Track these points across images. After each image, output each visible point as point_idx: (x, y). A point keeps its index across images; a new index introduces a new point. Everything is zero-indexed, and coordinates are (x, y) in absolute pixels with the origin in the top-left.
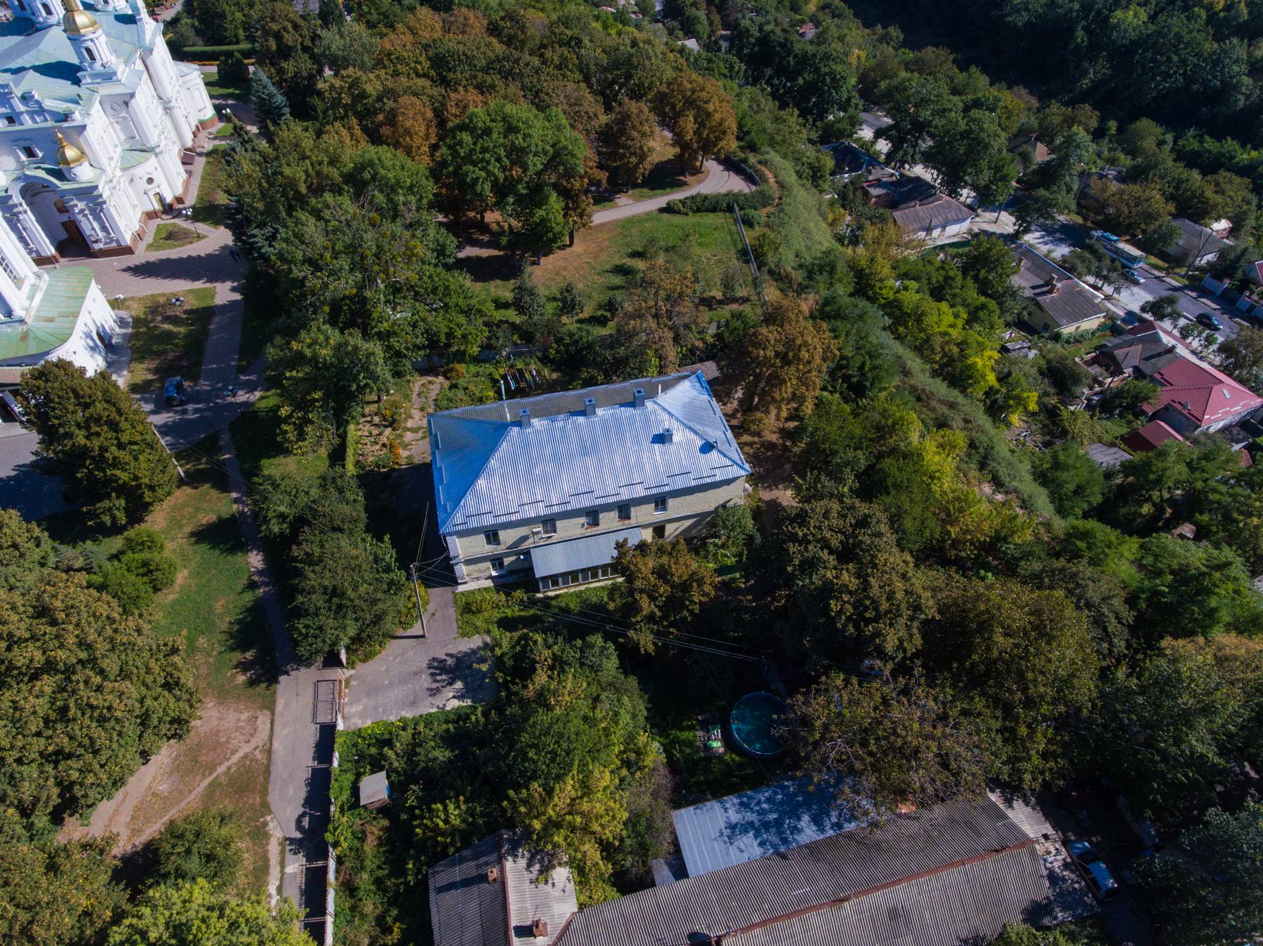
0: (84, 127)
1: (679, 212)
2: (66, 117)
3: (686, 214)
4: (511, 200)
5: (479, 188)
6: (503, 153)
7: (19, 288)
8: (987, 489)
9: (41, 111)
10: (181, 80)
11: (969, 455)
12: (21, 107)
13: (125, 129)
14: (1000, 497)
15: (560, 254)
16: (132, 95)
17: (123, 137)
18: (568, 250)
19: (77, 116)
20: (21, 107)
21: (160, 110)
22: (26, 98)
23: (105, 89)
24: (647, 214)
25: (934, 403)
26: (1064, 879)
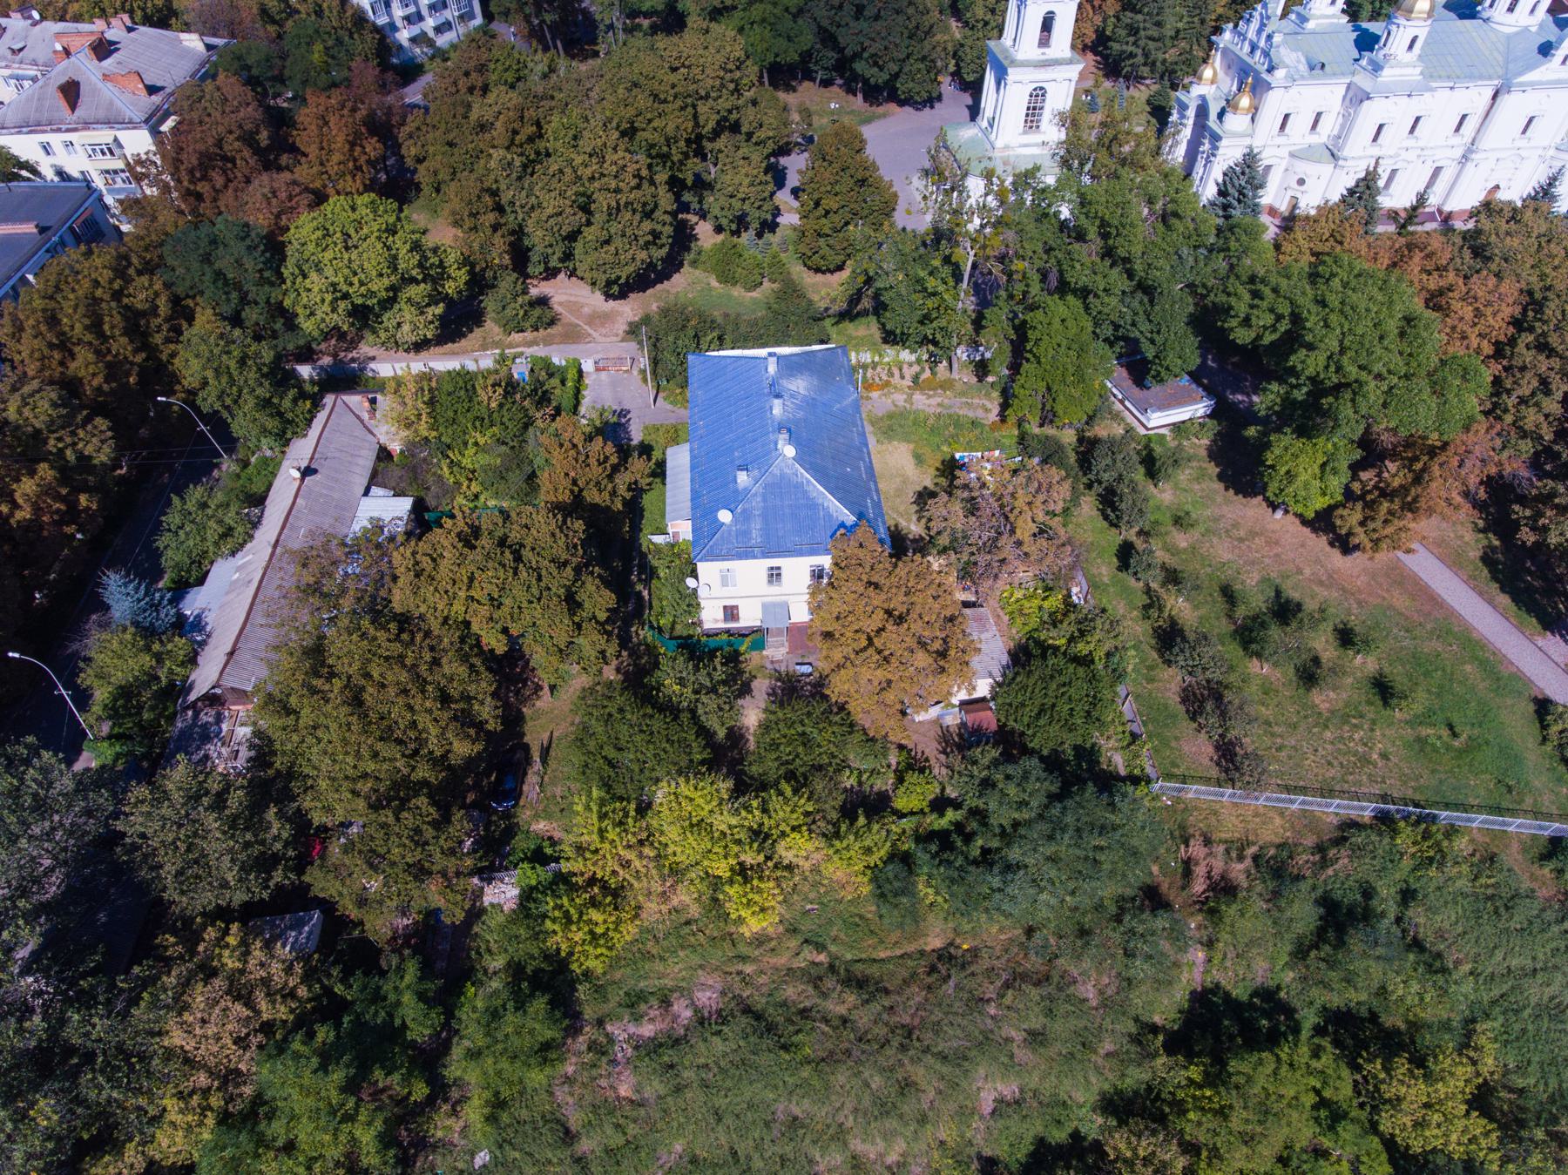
0: (1269, 87)
1: (1544, 727)
2: (1270, 70)
3: (1545, 739)
4: (1274, 387)
5: (1234, 323)
6: (1284, 309)
7: (1025, 133)
8: (707, 998)
9: (1266, 54)
10: (1552, 152)
11: (784, 1004)
12: (1262, 44)
13: (1343, 126)
14: (683, 1012)
15: (1320, 542)
16: (1369, 98)
17: (1335, 132)
18: (1335, 553)
19: (1280, 73)
20: (1262, 44)
21: (1459, 153)
22: (1269, 37)
23: (1363, 81)
24: (1519, 676)
25: (916, 995)
26: (199, 748)
